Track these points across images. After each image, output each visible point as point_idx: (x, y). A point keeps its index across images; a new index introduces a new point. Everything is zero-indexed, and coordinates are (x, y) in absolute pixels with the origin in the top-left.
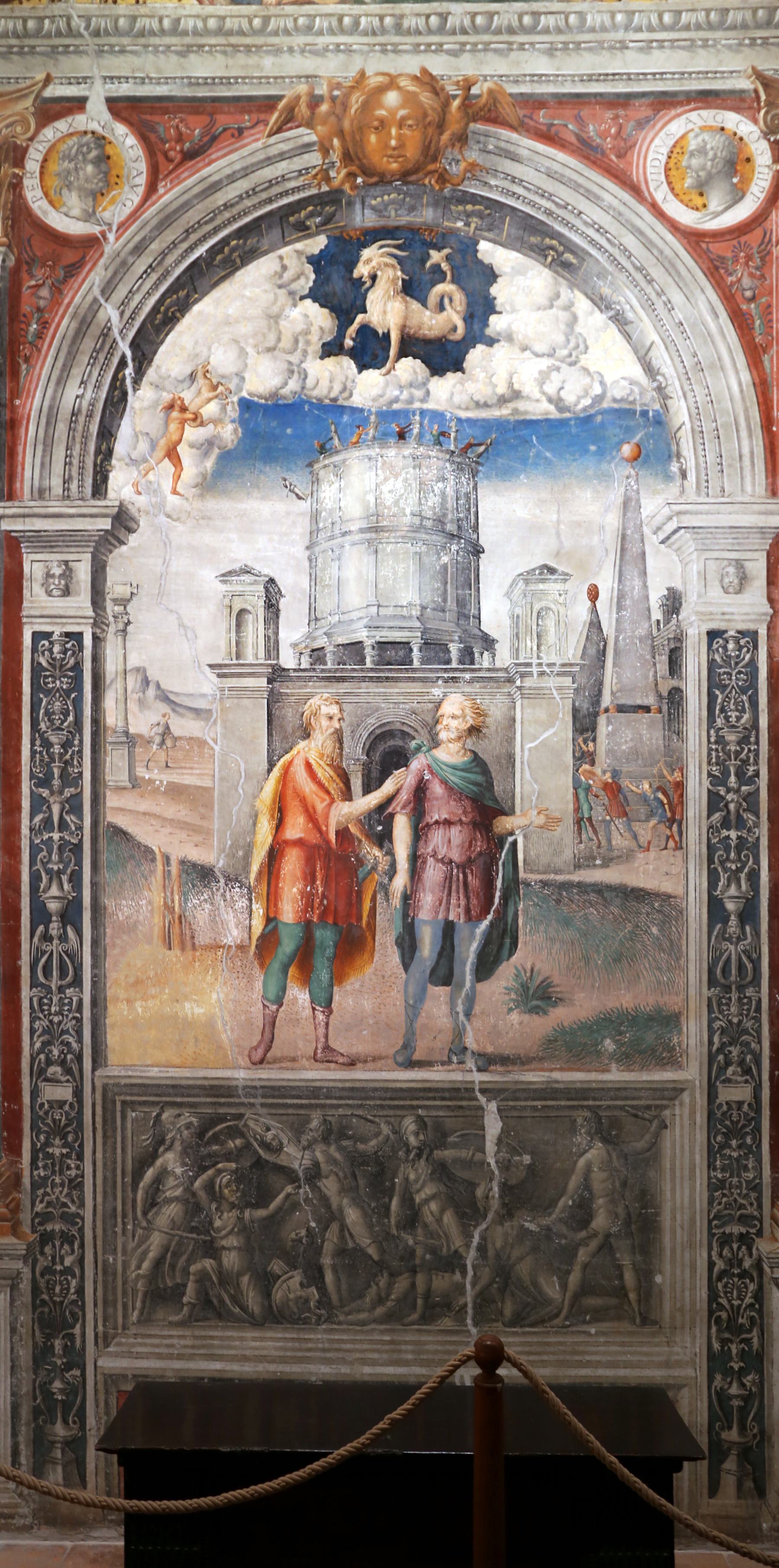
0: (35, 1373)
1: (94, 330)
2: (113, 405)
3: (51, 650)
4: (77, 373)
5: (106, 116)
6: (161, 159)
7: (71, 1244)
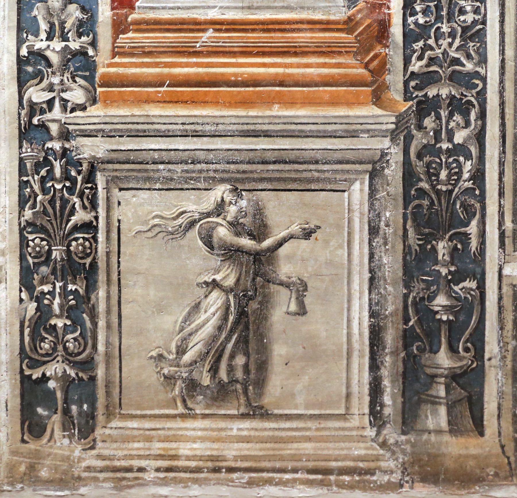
0: (407, 286)
7: (466, 114)
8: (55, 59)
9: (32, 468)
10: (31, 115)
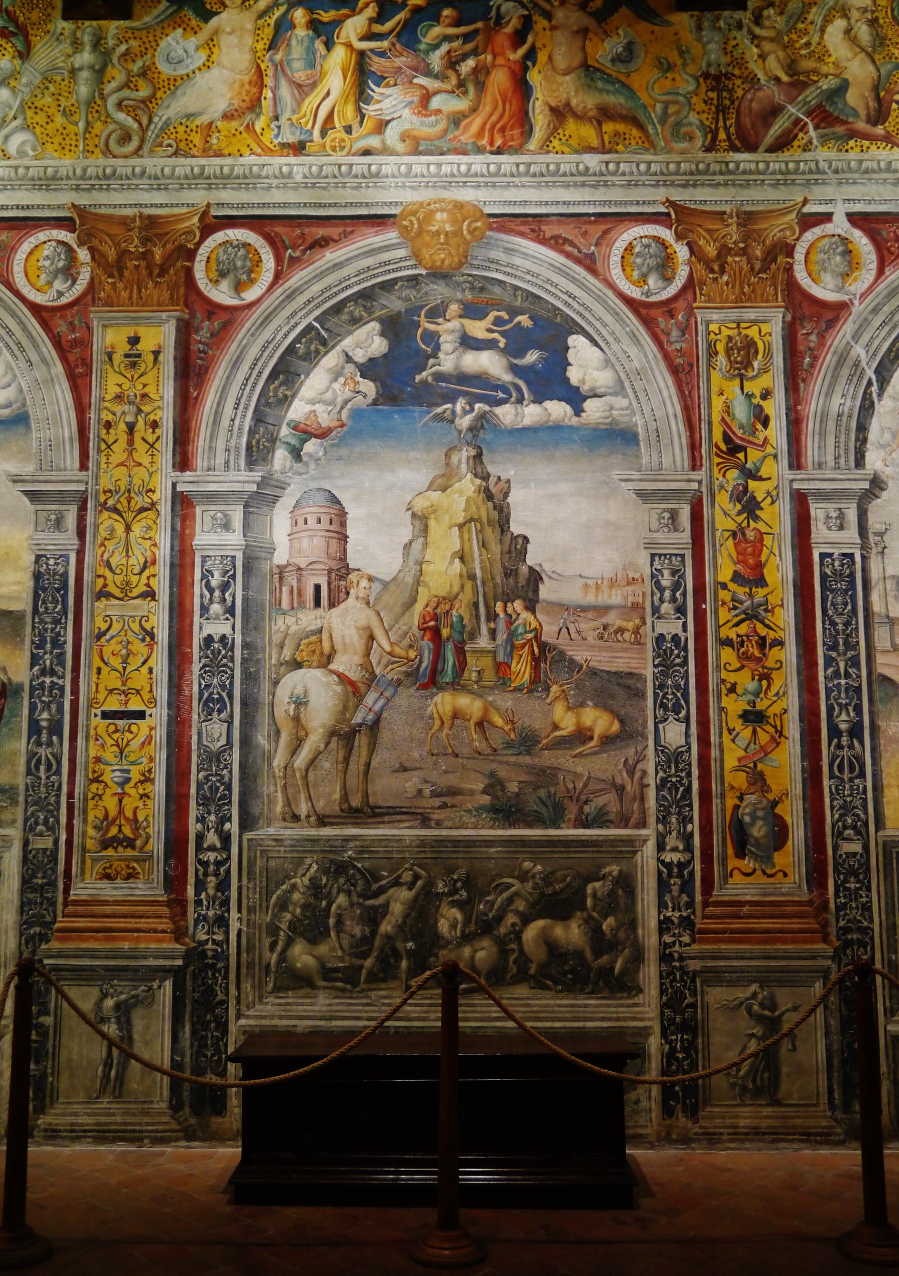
1: (849, 362)
2: (866, 410)
3: (833, 565)
4: (839, 389)
5: (847, 225)
6: (886, 253)
8: (676, 921)
9: (669, 1133)
10: (665, 949)
